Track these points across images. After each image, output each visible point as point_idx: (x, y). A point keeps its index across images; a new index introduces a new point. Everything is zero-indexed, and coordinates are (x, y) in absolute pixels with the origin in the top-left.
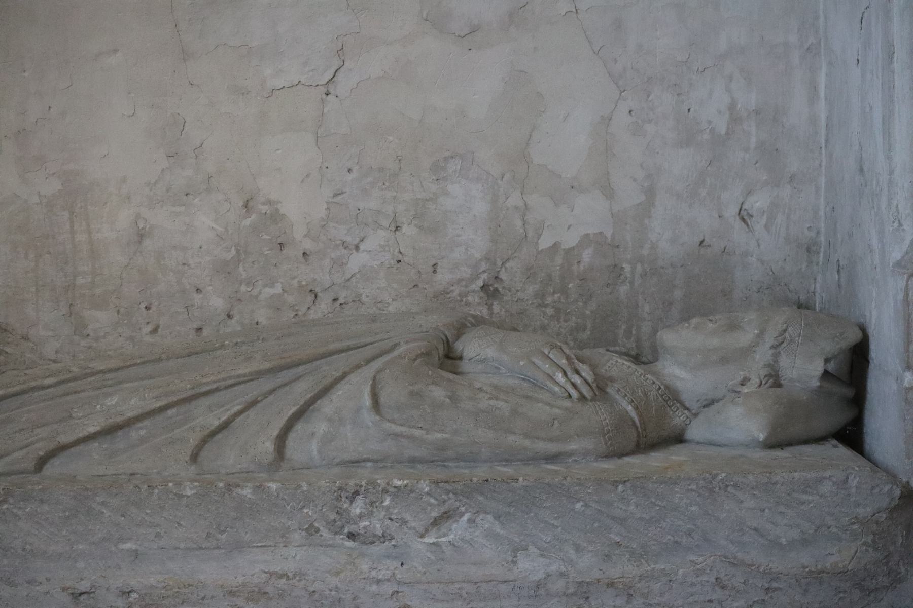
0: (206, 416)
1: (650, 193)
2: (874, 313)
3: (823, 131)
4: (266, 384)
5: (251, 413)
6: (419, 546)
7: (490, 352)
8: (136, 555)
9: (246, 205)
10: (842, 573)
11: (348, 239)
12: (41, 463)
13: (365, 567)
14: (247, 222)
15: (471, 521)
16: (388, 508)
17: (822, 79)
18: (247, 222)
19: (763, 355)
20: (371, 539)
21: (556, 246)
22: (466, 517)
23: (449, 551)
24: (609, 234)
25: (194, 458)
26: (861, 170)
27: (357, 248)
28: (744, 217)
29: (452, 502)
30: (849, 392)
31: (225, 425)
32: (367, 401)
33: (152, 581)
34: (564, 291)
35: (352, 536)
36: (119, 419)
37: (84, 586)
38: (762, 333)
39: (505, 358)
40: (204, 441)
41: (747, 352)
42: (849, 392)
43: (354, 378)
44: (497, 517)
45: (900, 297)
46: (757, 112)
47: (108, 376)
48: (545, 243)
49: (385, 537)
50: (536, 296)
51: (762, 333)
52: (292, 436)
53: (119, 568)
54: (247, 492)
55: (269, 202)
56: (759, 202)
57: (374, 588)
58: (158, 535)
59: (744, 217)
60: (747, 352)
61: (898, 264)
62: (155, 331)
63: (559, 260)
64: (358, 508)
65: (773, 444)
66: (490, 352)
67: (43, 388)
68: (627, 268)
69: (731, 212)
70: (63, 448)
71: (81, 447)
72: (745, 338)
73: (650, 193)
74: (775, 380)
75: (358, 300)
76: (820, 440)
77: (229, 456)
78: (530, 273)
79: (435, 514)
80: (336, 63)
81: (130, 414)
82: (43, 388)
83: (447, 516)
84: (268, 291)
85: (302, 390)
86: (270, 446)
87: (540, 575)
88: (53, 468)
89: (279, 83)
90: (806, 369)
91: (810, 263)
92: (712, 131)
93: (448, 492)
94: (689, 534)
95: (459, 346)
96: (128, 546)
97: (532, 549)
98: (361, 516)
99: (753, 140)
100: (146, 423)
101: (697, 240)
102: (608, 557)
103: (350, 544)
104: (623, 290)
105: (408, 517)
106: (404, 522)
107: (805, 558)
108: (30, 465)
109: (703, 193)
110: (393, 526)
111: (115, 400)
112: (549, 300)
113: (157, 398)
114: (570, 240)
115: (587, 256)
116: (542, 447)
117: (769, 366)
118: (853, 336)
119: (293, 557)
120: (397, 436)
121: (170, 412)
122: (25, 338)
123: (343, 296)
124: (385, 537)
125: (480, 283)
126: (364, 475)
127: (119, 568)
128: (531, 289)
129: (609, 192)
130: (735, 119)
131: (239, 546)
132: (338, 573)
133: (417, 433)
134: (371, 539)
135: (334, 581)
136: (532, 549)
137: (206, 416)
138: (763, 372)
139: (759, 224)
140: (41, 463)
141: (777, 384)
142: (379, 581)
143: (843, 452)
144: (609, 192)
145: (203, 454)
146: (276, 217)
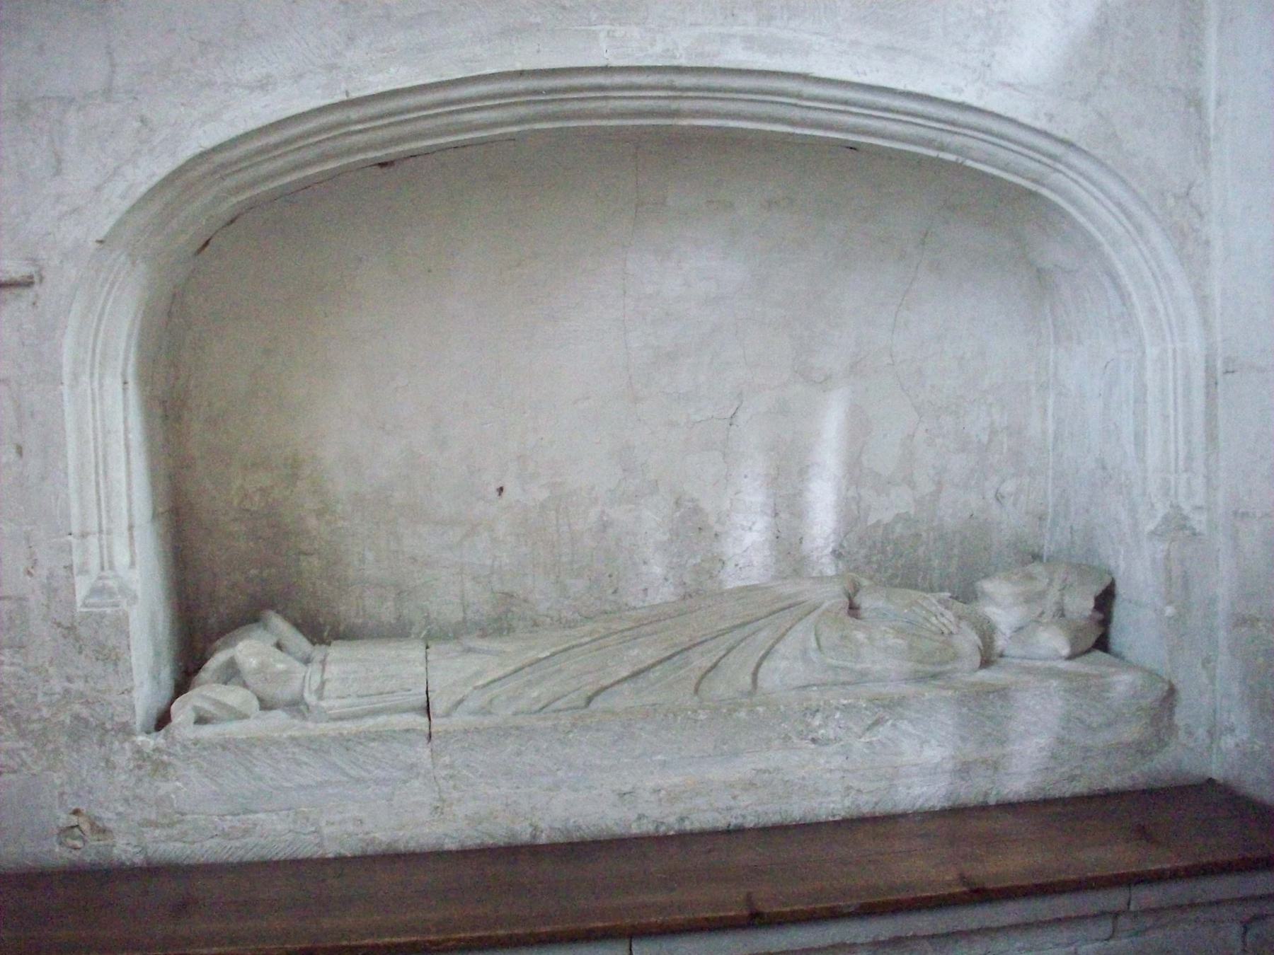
0: (700, 661)
1: (939, 484)
2: (1122, 565)
3: (1050, 439)
4: (738, 634)
5: (731, 656)
6: (859, 745)
7: (881, 604)
8: (664, 764)
9: (677, 503)
10: (1128, 745)
11: (745, 523)
12: (589, 700)
13: (822, 761)
14: (678, 514)
15: (894, 725)
16: (838, 720)
17: (1050, 402)
18: (678, 514)
19: (1053, 595)
20: (827, 742)
21: (879, 521)
22: (890, 723)
23: (878, 747)
24: (912, 512)
25: (696, 691)
26: (1104, 468)
27: (750, 529)
28: (999, 498)
29: (881, 712)
30: (1099, 616)
31: (714, 666)
32: (814, 645)
33: (676, 780)
34: (884, 552)
35: (814, 740)
36: (641, 666)
37: (627, 788)
38: (1051, 580)
39: (892, 607)
40: (703, 677)
41: (1042, 595)
42: (1099, 616)
43: (799, 627)
44: (911, 721)
45: (1159, 556)
46: (1007, 428)
47: (626, 633)
48: (872, 520)
49: (837, 739)
50: (866, 557)
51: (1051, 580)
52: (761, 670)
53: (652, 773)
54: (742, 714)
55: (692, 500)
56: (1009, 487)
57: (828, 775)
58: (680, 749)
59: (999, 498)
60: (1042, 595)
61: (1153, 533)
62: (615, 592)
63: (880, 531)
64: (817, 722)
65: (1071, 657)
66: (881, 604)
67: (581, 645)
68: (924, 535)
69: (990, 495)
70: (605, 689)
71: (616, 688)
72: (1040, 585)
73: (939, 484)
74: (1061, 612)
75: (750, 565)
76: (1088, 651)
77: (720, 688)
78: (861, 541)
79: (869, 722)
80: (736, 404)
81: (650, 662)
82: (581, 645)
83: (877, 723)
84: (692, 561)
85: (764, 637)
86: (748, 679)
87: (938, 759)
88: (598, 703)
89: (698, 418)
90: (1082, 604)
91: (1040, 526)
92: (979, 442)
93: (878, 706)
94: (1035, 724)
95: (857, 600)
96: (659, 757)
97: (933, 742)
98: (820, 727)
99: (1005, 447)
100: (658, 667)
101: (968, 514)
102: (983, 743)
103: (813, 746)
104: (921, 550)
105: (851, 725)
106: (849, 729)
107: (1106, 737)
108: (582, 703)
109: (973, 483)
110: (841, 733)
111: (636, 651)
112: (874, 559)
113: (666, 649)
114: (887, 517)
115: (899, 529)
116: (929, 668)
117: (1057, 603)
118: (1107, 581)
119: (775, 757)
120: (835, 668)
121: (675, 659)
122: (525, 601)
123: (742, 562)
124: (837, 739)
125: (830, 549)
126: (814, 694)
127: (652, 773)
128: (863, 552)
129: (912, 485)
130: (993, 433)
131: (736, 754)
132: (803, 767)
133: (849, 664)
134: (827, 742)
135: (802, 773)
136: (933, 742)
137: (700, 661)
138: (1054, 609)
139: (1008, 502)
140: (589, 700)
141: (1063, 615)
142: (831, 771)
143: (1099, 654)
144: (912, 485)
145: (704, 686)
146: (697, 510)
